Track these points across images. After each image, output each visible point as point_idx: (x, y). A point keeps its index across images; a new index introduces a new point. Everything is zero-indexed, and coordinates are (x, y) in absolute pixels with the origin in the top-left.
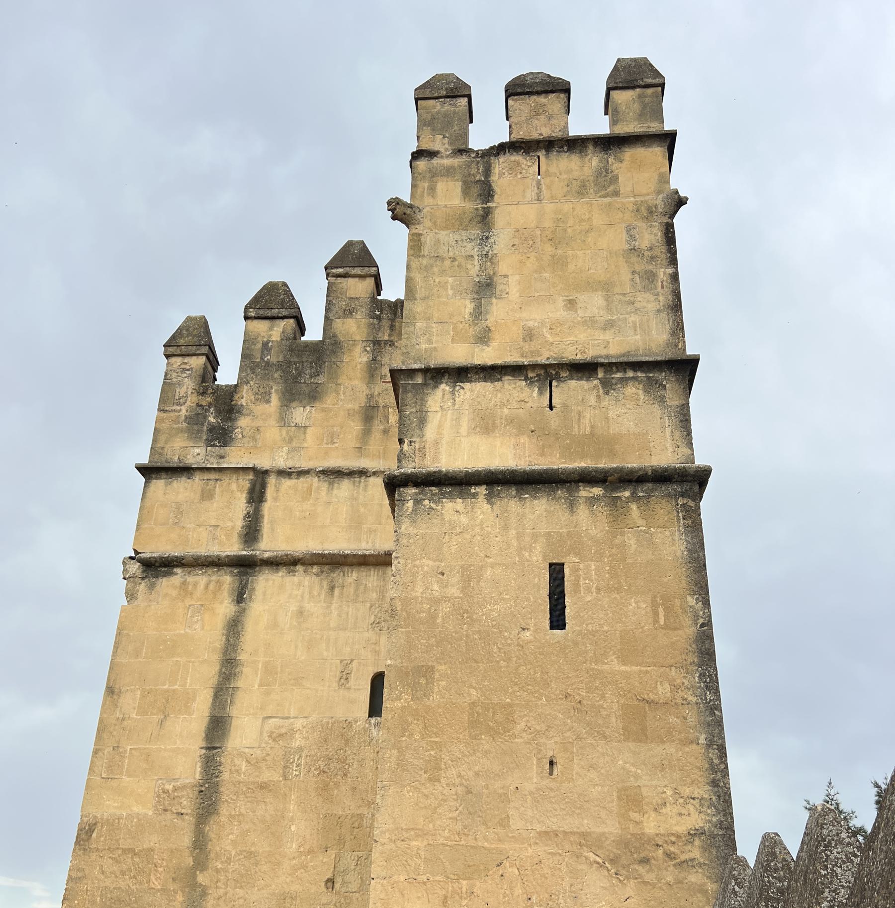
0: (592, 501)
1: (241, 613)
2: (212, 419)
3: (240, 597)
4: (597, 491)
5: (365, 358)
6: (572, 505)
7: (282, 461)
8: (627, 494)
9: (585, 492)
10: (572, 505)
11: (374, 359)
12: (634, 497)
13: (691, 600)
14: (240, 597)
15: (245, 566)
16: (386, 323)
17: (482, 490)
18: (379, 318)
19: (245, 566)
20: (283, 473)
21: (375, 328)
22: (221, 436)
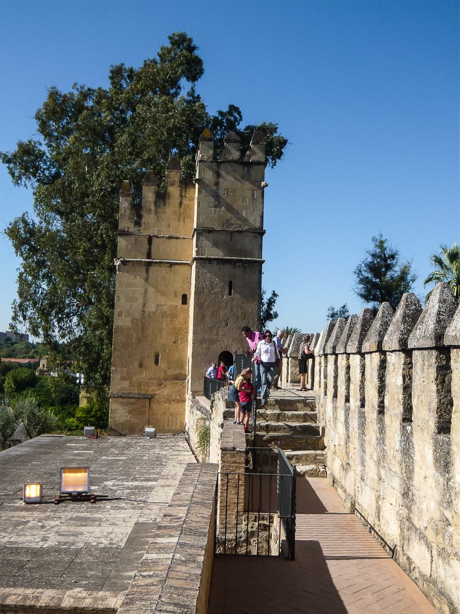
0: (239, 266)
1: (148, 276)
2: (135, 218)
3: (147, 272)
4: (241, 264)
5: (179, 201)
6: (235, 267)
7: (156, 233)
8: (247, 265)
9: (237, 264)
10: (235, 267)
11: (181, 201)
12: (249, 266)
13: (258, 291)
14: (147, 272)
15: (149, 264)
16: (184, 189)
17: (216, 262)
18: (181, 187)
19: (149, 264)
20: (156, 236)
21: (181, 191)
22: (138, 224)
